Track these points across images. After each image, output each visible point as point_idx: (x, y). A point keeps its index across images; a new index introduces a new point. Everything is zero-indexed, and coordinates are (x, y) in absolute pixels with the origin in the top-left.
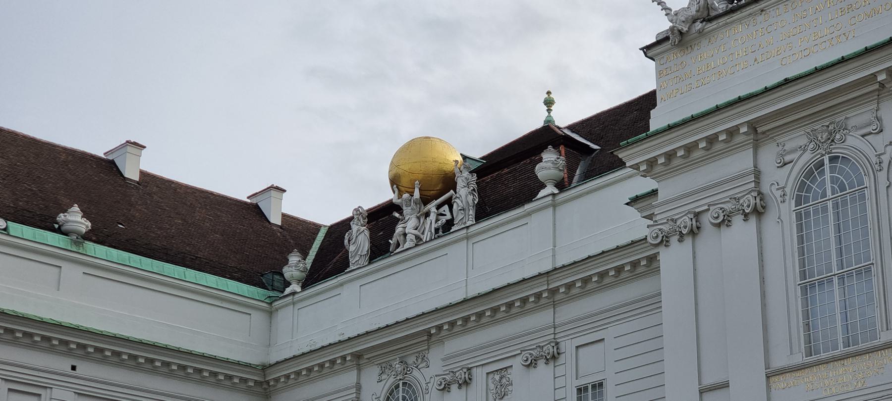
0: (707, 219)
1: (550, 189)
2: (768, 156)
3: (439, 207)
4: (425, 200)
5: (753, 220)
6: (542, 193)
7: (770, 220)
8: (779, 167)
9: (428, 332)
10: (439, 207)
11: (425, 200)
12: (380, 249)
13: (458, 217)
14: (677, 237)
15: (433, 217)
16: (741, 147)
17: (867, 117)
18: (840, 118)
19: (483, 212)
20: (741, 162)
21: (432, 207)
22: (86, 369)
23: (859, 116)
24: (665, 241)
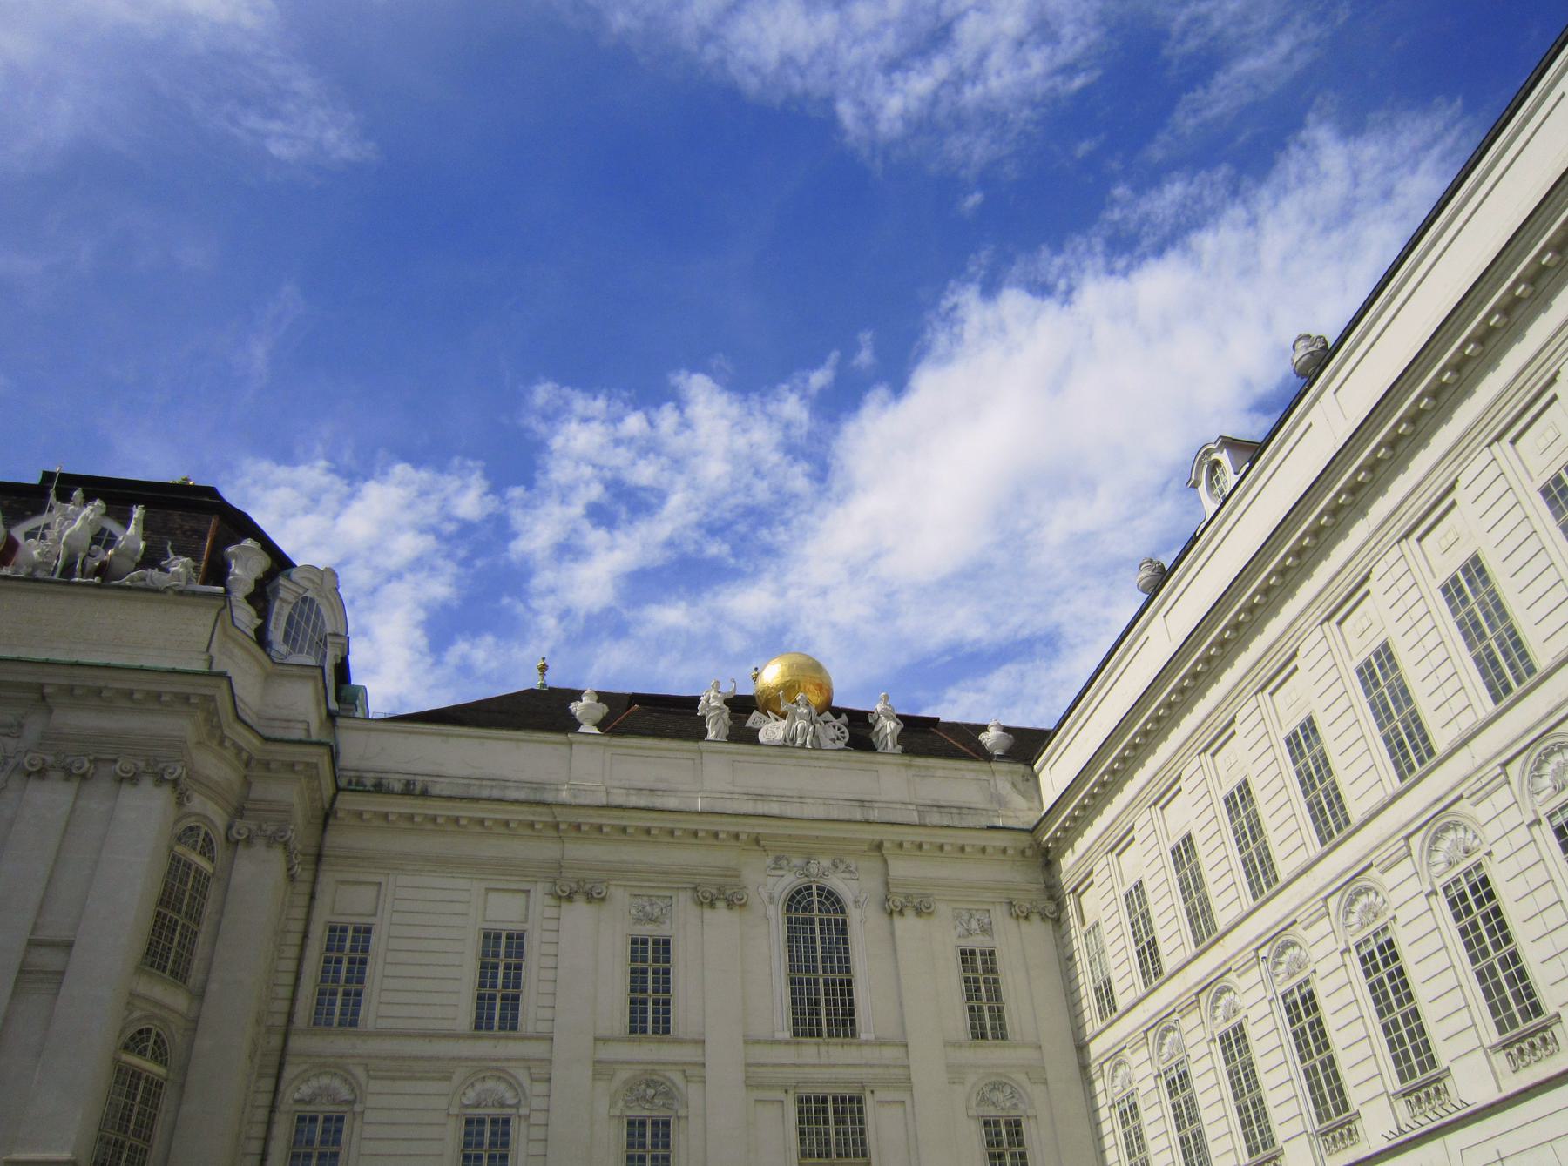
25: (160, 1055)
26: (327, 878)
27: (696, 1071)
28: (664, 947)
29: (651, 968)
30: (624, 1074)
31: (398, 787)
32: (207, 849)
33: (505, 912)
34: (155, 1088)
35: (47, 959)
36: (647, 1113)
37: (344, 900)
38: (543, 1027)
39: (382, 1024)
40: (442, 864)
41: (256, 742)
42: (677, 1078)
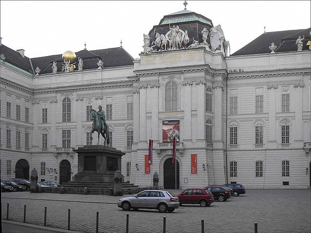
0: (149, 86)
1: (100, 68)
2: (161, 78)
3: (73, 65)
4: (70, 64)
5: (158, 88)
6: (98, 68)
7: (160, 88)
8: (163, 80)
9: (74, 90)
10: (73, 65)
11: (70, 64)
12: (59, 70)
13: (79, 69)
14: (143, 88)
15: (72, 67)
16: (157, 75)
17: (178, 76)
18: (174, 75)
19: (84, 68)
20: (155, 78)
21: (72, 65)
22: (8, 88)
23: (177, 76)
24: (141, 88)
25: (211, 123)
26: (229, 89)
27: (294, 118)
28: (288, 95)
29: (286, 99)
30: (281, 119)
31: (238, 71)
32: (211, 91)
33: (259, 92)
34: (211, 127)
35: (194, 113)
36: (285, 125)
37: (232, 93)
38: (267, 112)
39: (241, 113)
40: (248, 85)
41: (214, 71)
42: (290, 119)
